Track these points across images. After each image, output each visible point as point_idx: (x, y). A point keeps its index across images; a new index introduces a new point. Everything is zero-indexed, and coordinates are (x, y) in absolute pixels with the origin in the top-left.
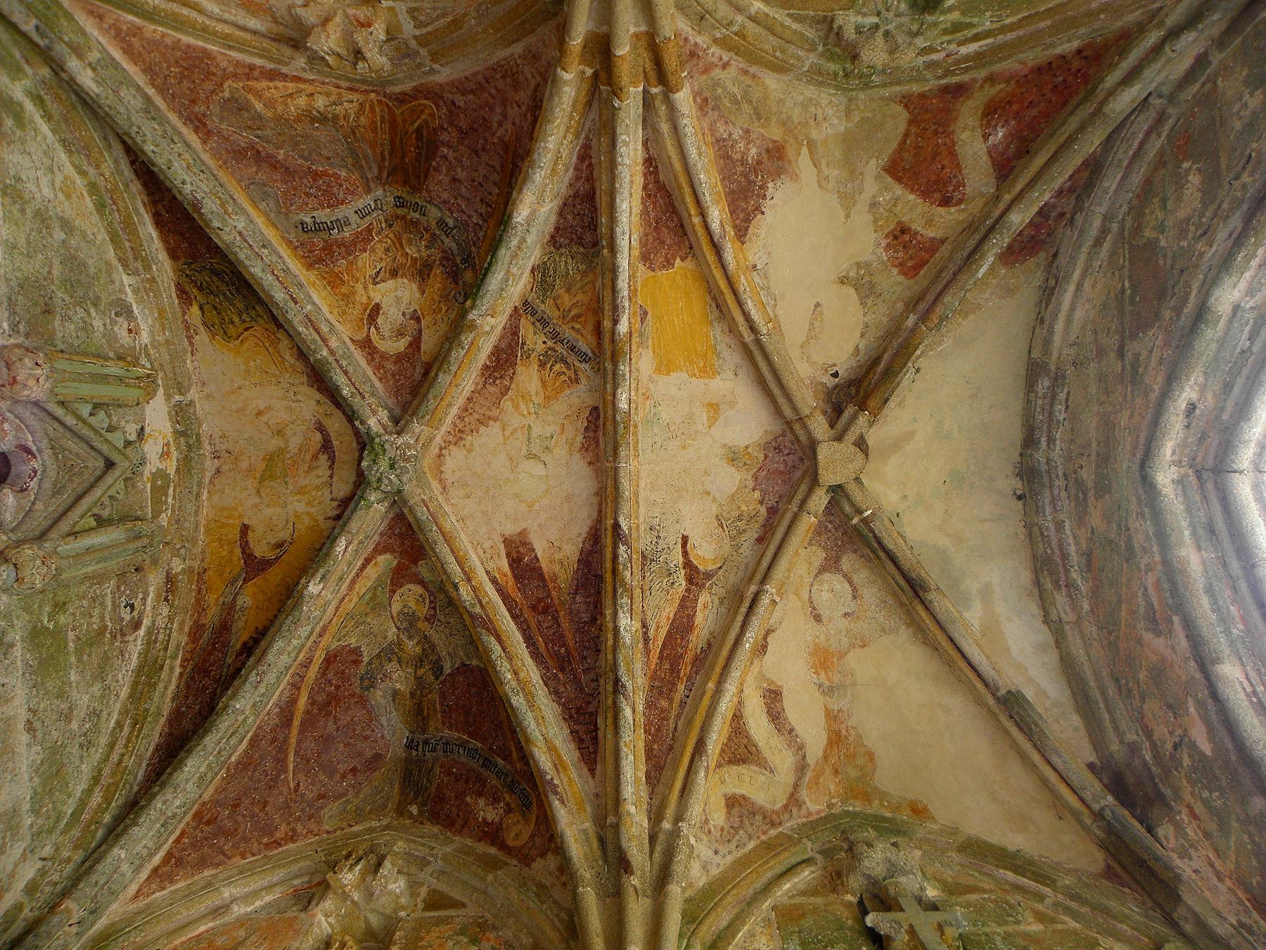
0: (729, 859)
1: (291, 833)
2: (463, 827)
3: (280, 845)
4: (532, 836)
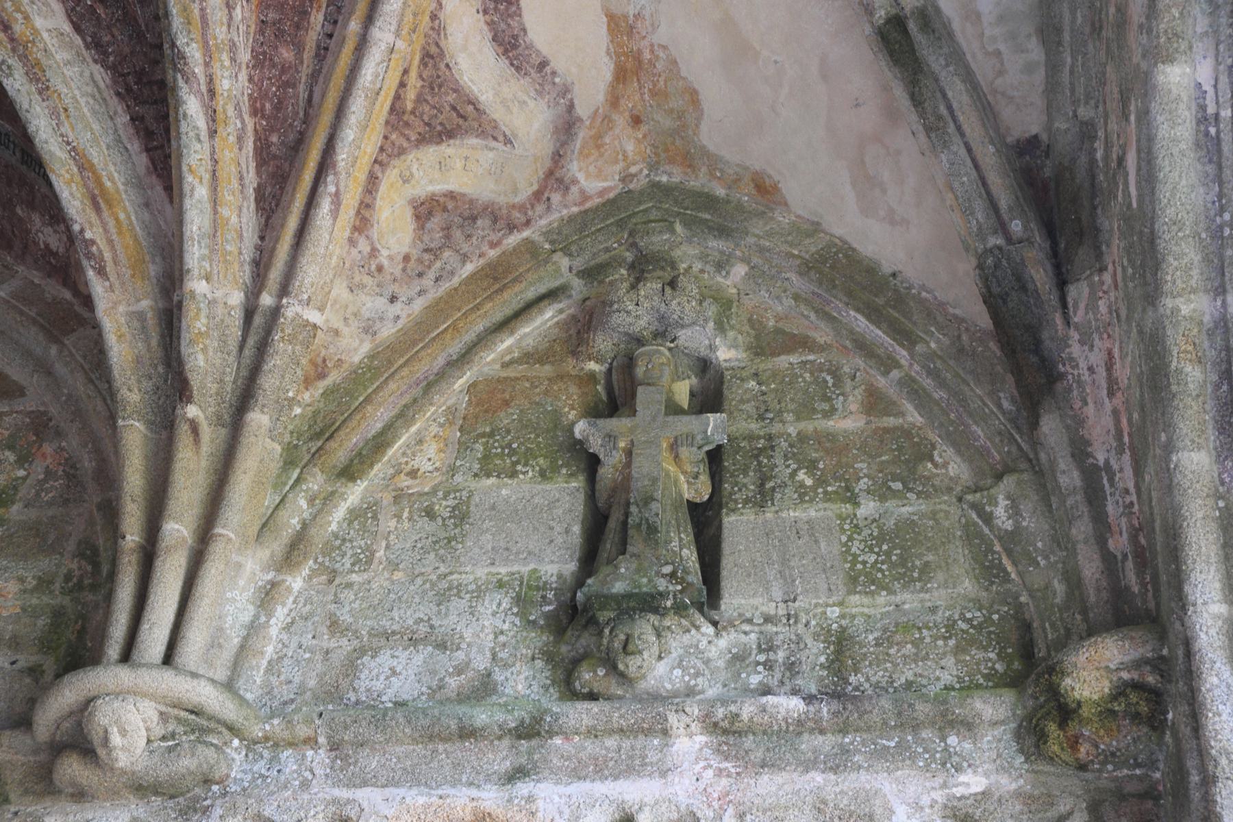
0: (419, 305)
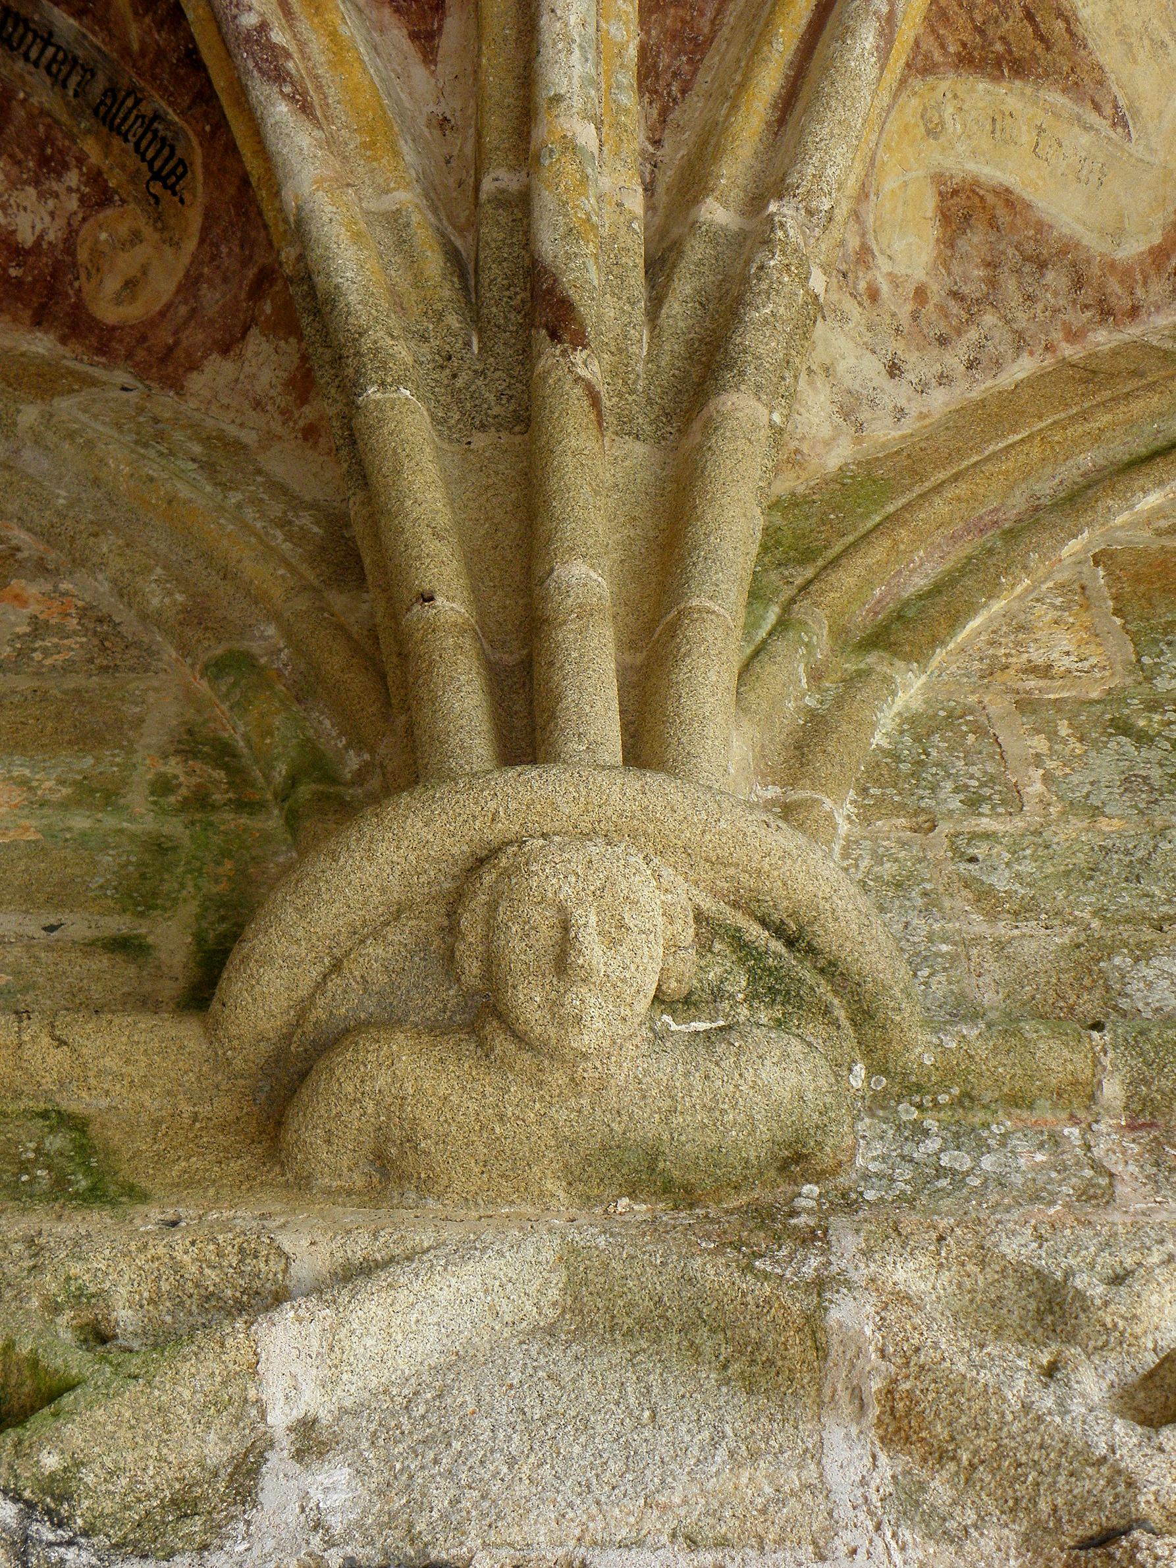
0: (939, 401)
4: (190, 284)
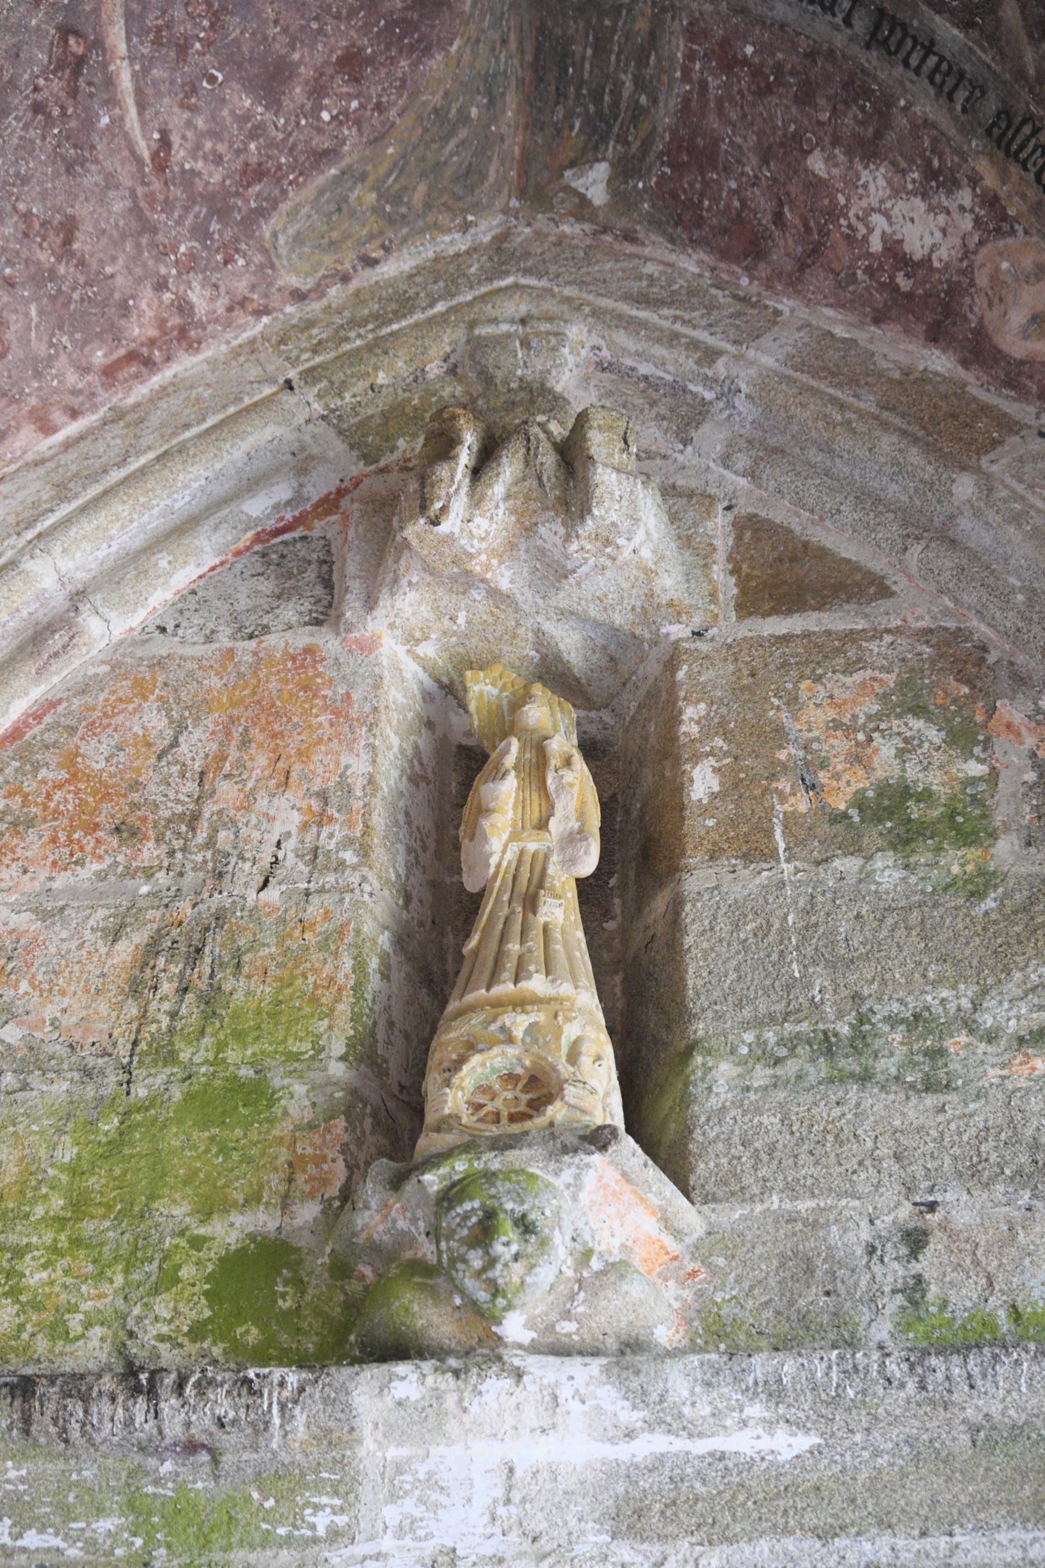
1: (175, 321)
2: (802, 267)
3: (149, 363)
